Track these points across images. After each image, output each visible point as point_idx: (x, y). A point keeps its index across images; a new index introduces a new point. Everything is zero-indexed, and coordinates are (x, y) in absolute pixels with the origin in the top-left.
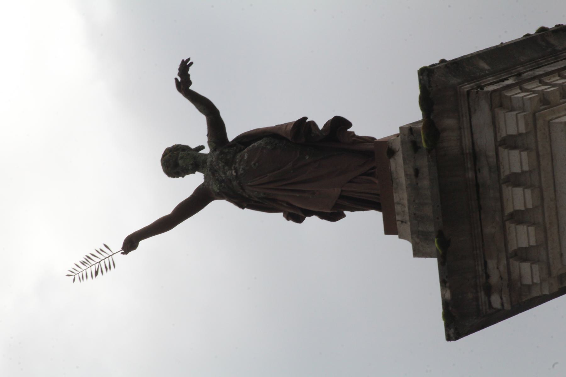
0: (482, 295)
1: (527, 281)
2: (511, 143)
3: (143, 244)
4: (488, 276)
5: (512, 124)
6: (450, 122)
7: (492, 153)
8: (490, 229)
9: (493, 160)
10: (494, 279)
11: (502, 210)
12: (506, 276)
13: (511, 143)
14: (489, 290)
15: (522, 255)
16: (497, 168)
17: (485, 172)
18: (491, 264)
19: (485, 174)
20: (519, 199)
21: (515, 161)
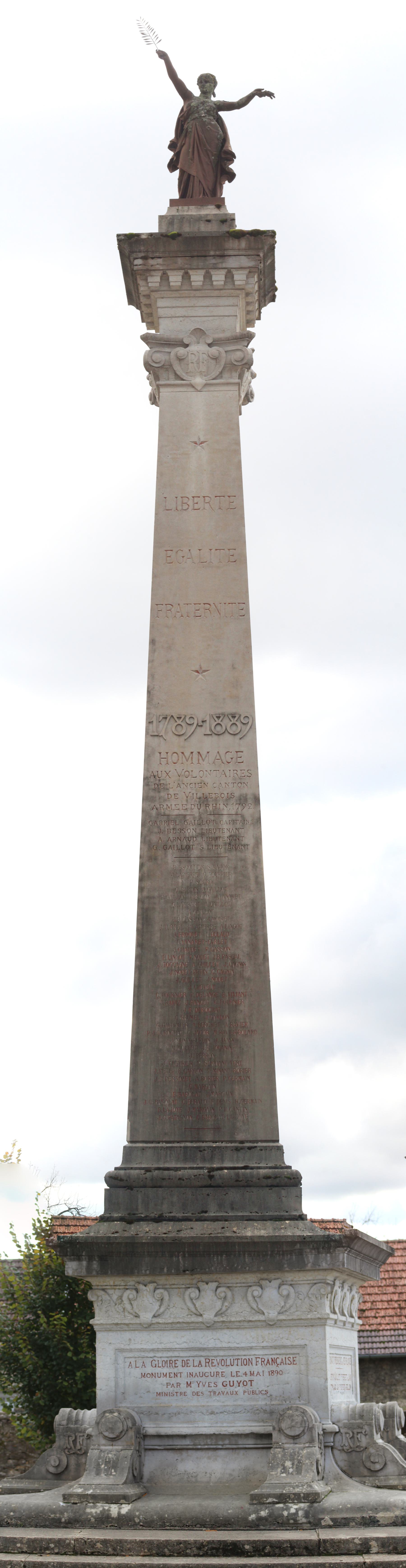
0: (143, 254)
1: (150, 279)
2: (229, 275)
3: (162, 62)
4: (153, 258)
5: (240, 277)
7: (224, 265)
8: (180, 261)
9: (220, 266)
10: (151, 262)
11: (191, 269)
12: (153, 268)
13: (229, 275)
14: (145, 258)
15: (165, 277)
16: (215, 268)
17: (213, 261)
18: (160, 261)
20: (197, 278)
21: (219, 277)
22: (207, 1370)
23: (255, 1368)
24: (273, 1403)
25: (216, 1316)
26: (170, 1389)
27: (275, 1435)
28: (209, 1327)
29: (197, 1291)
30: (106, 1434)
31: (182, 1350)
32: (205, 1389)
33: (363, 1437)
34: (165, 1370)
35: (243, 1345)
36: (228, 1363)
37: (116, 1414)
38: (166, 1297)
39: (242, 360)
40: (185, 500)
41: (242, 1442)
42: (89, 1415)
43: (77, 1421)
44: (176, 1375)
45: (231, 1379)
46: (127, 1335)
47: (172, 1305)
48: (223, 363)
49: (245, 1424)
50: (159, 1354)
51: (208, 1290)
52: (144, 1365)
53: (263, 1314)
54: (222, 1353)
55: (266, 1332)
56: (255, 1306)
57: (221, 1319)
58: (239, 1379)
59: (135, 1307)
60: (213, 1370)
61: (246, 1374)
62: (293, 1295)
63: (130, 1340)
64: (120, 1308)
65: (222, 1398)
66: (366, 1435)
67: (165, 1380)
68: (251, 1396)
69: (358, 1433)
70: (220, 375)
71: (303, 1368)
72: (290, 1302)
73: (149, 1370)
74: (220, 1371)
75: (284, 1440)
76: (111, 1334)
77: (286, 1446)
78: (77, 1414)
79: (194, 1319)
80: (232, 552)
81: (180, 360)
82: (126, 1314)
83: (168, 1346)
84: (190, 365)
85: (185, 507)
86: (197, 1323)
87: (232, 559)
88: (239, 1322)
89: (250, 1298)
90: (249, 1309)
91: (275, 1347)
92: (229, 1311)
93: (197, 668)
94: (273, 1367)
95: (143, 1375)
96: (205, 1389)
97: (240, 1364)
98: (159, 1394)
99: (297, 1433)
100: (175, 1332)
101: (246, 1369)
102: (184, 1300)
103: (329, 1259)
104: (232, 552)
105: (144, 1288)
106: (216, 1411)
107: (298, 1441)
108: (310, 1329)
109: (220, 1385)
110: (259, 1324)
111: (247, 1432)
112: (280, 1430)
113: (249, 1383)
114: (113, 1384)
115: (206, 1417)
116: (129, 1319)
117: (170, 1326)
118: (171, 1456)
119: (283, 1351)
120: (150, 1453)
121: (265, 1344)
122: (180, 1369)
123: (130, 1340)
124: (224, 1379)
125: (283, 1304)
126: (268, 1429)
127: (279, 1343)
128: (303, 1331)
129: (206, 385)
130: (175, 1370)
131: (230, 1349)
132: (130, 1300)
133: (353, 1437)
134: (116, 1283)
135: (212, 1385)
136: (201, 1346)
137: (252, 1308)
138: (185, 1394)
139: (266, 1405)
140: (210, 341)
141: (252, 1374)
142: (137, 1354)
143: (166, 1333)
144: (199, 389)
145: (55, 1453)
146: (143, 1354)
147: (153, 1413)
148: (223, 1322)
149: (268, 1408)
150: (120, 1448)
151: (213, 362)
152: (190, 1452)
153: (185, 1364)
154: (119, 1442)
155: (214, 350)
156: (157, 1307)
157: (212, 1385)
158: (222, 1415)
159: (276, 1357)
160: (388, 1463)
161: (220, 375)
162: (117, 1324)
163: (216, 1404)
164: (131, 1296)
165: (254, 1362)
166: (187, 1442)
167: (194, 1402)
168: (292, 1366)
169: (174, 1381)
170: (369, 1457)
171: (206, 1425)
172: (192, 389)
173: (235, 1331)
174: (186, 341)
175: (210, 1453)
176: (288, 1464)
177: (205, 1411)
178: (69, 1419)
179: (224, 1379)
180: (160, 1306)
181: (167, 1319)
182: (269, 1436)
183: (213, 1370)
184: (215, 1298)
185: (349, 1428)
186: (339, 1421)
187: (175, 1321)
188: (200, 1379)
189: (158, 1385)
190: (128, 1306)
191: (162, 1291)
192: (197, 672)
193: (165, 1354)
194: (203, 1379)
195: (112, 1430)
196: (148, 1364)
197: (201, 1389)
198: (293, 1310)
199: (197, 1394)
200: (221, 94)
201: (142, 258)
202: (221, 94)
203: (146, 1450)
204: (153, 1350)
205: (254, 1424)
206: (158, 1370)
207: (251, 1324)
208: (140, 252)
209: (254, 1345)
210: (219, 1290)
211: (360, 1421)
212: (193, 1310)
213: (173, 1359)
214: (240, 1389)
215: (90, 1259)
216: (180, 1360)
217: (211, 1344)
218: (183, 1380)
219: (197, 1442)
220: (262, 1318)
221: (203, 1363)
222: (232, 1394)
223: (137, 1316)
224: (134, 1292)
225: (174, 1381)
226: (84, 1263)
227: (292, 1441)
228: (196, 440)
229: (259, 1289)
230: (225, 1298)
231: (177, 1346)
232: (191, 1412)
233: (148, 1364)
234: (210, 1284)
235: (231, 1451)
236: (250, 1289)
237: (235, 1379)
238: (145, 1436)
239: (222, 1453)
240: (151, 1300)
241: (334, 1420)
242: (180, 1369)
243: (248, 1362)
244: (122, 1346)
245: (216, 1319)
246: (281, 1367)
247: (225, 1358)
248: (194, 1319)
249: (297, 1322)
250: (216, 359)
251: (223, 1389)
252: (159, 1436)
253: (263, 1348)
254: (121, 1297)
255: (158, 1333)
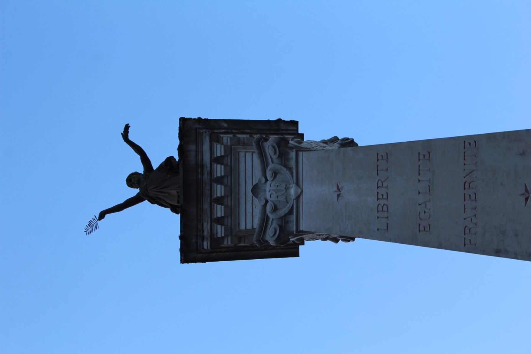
0: (200, 241)
1: (219, 236)
2: (219, 160)
4: (203, 231)
5: (219, 151)
6: (193, 147)
7: (209, 165)
8: (206, 206)
9: (209, 169)
10: (205, 233)
11: (211, 196)
12: (209, 231)
13: (219, 160)
14: (203, 239)
15: (220, 221)
16: (211, 172)
17: (206, 174)
19: (206, 177)
39: (274, 147)
40: (380, 208)
48: (279, 167)
70: (290, 169)
80: (421, 157)
81: (275, 209)
84: (280, 199)
85: (385, 208)
87: (427, 157)
93: (523, 199)
104: (421, 157)
129: (297, 184)
140: (263, 180)
144: (300, 191)
151: (278, 176)
155: (269, 174)
161: (290, 169)
172: (301, 197)
174: (263, 203)
192: (527, 199)
200: (140, 169)
201: (203, 241)
202: (140, 169)
208: (197, 243)
228: (335, 195)
250: (275, 174)
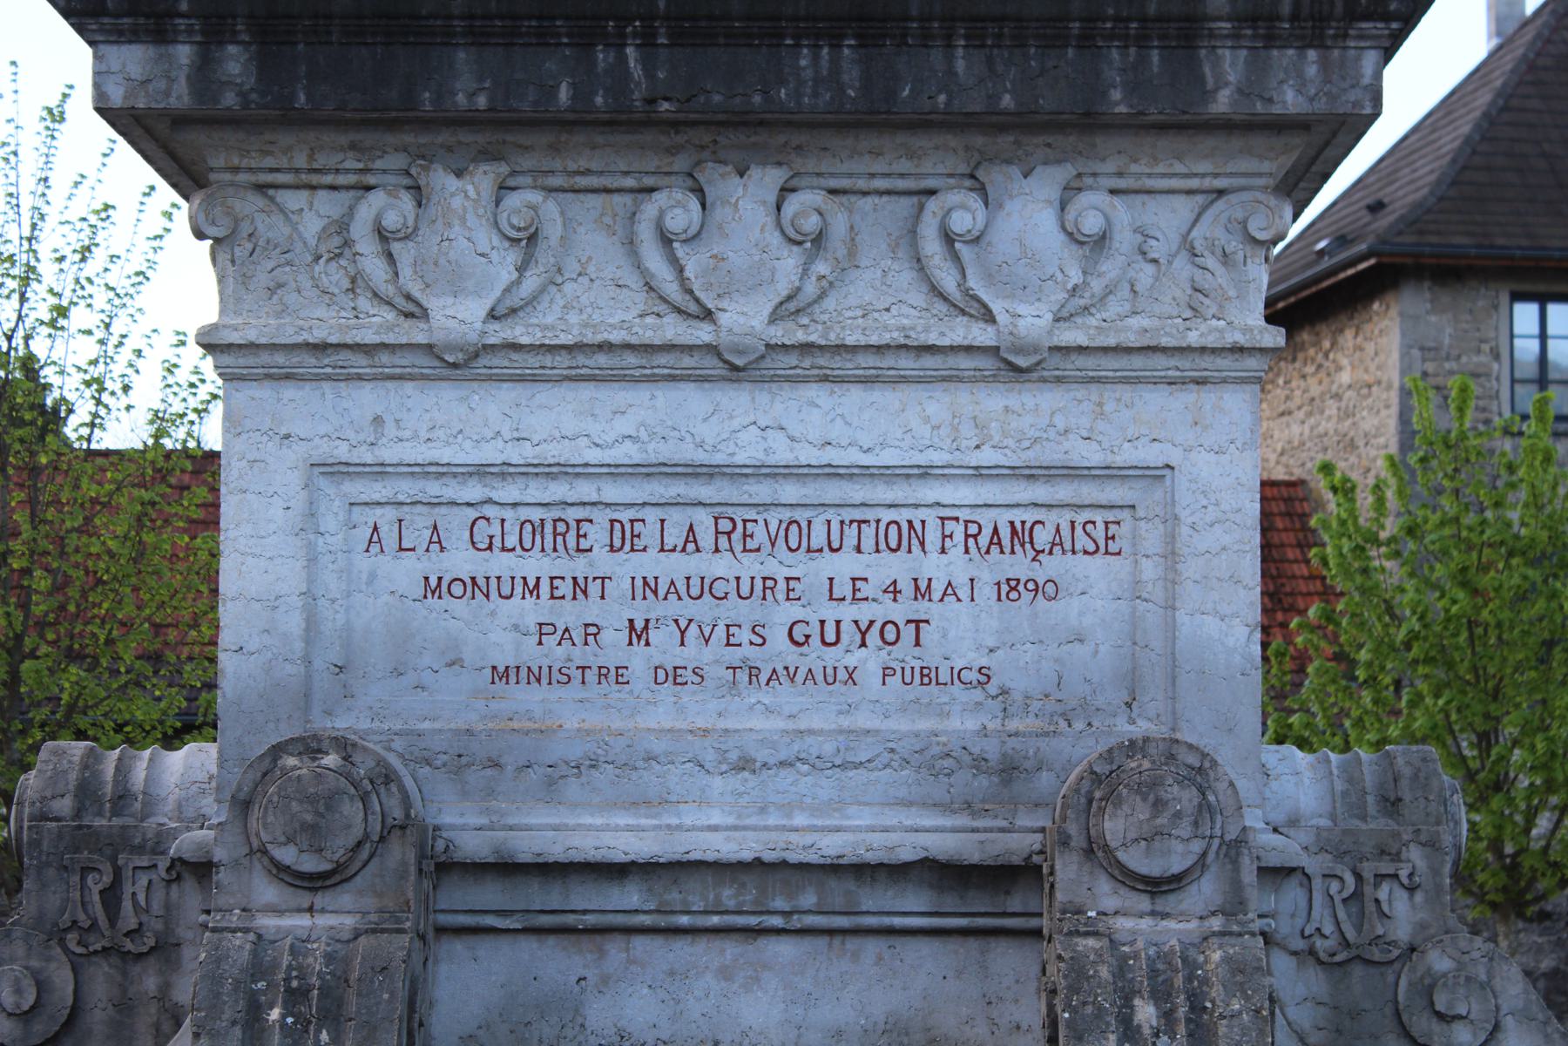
22: (722, 566)
23: (934, 567)
24: (1014, 725)
25: (774, 318)
26: (555, 653)
27: (1067, 871)
28: (735, 368)
29: (694, 205)
30: (287, 855)
31: (615, 472)
32: (711, 656)
33: (1401, 895)
34: (535, 565)
35: (888, 457)
36: (818, 539)
37: (331, 760)
38: (553, 231)
41: (878, 901)
42: (184, 769)
43: (122, 798)
44: (580, 588)
45: (830, 612)
46: (367, 399)
47: (572, 267)
49: (891, 818)
50: (509, 492)
51: (747, 199)
52: (437, 539)
53: (989, 317)
54: (790, 492)
55: (994, 401)
56: (948, 280)
57: (801, 336)
58: (864, 613)
59: (406, 272)
60: (750, 567)
61: (894, 590)
62: (1124, 239)
63: (378, 421)
64: (335, 277)
65: (784, 695)
66: (1411, 890)
67: (530, 611)
68: (917, 690)
69: (1380, 878)
71: (1150, 570)
72: (1110, 268)
73: (461, 561)
74: (781, 573)
75: (1107, 895)
76: (289, 391)
77: (1124, 924)
78: (122, 769)
79: (673, 329)
82: (364, 303)
83: (555, 452)
86: (689, 349)
88: (879, 349)
89: (932, 246)
90: (918, 298)
91: (1029, 474)
92: (830, 303)
94: (1018, 565)
95: (434, 588)
96: (711, 656)
97: (868, 543)
98: (502, 674)
99: (1176, 868)
100: (587, 391)
101: (895, 567)
102: (631, 245)
103: (1312, 70)
105: (452, 183)
106: (762, 755)
107: (1169, 903)
108: (1190, 396)
109: (778, 639)
110: (965, 362)
111: (907, 855)
112: (1095, 851)
113: (908, 632)
114: (293, 623)
115: (718, 782)
116: (377, 324)
117: (562, 360)
118: (556, 964)
119: (1063, 492)
120: (458, 946)
121: (987, 457)
122: (602, 561)
123: (378, 421)
124: (795, 611)
125: (1075, 277)
126: (1017, 845)
127: (1049, 454)
128: (1154, 401)
130: (580, 567)
131: (832, 473)
132: (383, 235)
133: (1357, 895)
134: (321, 161)
135: (744, 635)
136: (701, 457)
137: (937, 292)
138: (619, 675)
139: (984, 732)
141: (922, 591)
142: (406, 489)
143: (545, 394)
145: (19, 949)
146: (434, 489)
147: (474, 761)
148: (807, 348)
149: (992, 749)
150: (349, 921)
152: (640, 943)
153: (625, 538)
154: (345, 898)
156: (506, 274)
157: (744, 635)
158: (785, 777)
159: (1030, 516)
160: (1509, 1022)
162: (322, 348)
163: (758, 723)
164: (391, 220)
165: (933, 537)
166: (630, 896)
167: (662, 713)
168: (1099, 559)
169: (571, 614)
170: (1429, 993)
171: (716, 818)
173: (856, 393)
175: (731, 949)
176: (1146, 1013)
177: (709, 757)
178: (86, 792)
179: (795, 611)
180: (521, 269)
181: (553, 321)
182: (1022, 874)
183: (750, 567)
184: (775, 239)
185: (1340, 856)
186: (1293, 822)
187: (590, 338)
188: (688, 608)
189: (502, 631)
190: (375, 268)
191: (535, 197)
193: (535, 491)
194: (704, 609)
195: (312, 834)
196: (456, 536)
197: (693, 652)
198: (1114, 308)
199: (674, 675)
203: (441, 930)
204: (481, 472)
205: (928, 822)
206: (500, 564)
207: (929, 361)
209: (937, 458)
210: (793, 205)
211: (1379, 824)
212: (672, 290)
213: (572, 514)
214: (869, 661)
215: (214, 33)
216: (602, 517)
217: (748, 450)
218: (613, 614)
219: (674, 897)
220: (982, 335)
221: (706, 538)
222: (831, 678)
223: (415, 311)
224: (407, 201)
225: (571, 614)
226: (184, 53)
227: (1144, 903)
229: (974, 201)
230: (819, 239)
231: (593, 456)
232: (651, 758)
233: (456, 536)
234: (755, 172)
235: (822, 942)
236: (932, 205)
237: (848, 612)
238: (446, 867)
239: (784, 949)
240: (485, 238)
241: (1278, 817)
242: (602, 561)
243: (909, 537)
244: (342, 452)
245: (778, 334)
246: (1053, 566)
247: (801, 515)
248: (673, 329)
249: (1138, 361)
251: (791, 655)
252: (507, 869)
253: (979, 473)
254: (341, 227)
255: (508, 393)
